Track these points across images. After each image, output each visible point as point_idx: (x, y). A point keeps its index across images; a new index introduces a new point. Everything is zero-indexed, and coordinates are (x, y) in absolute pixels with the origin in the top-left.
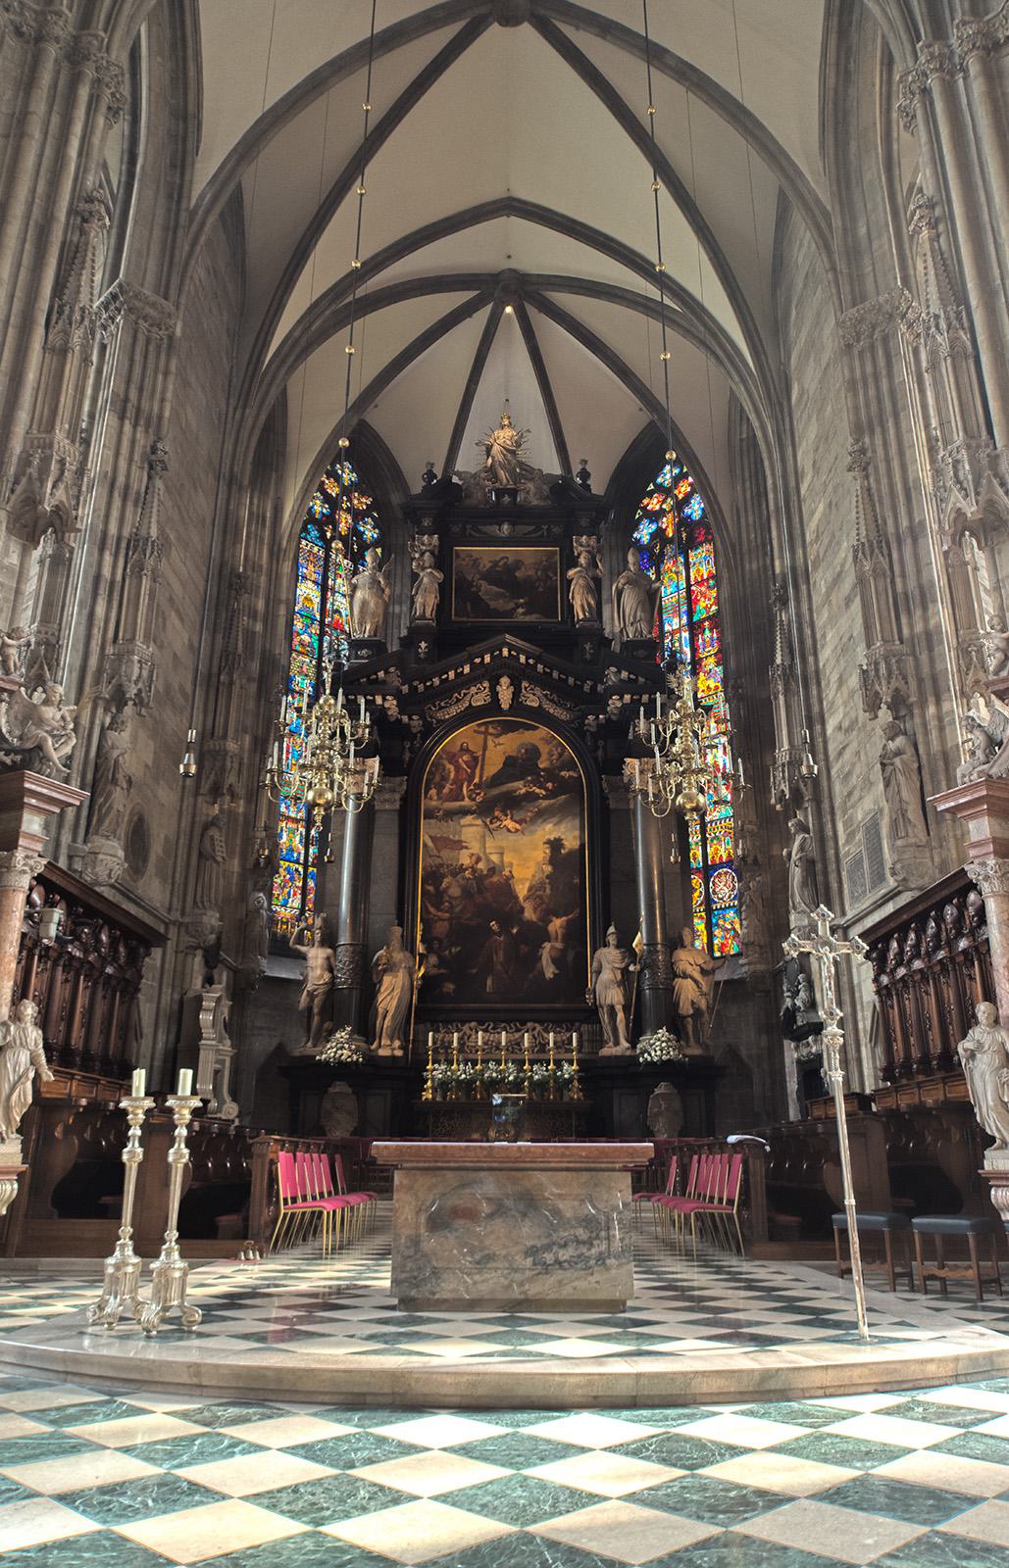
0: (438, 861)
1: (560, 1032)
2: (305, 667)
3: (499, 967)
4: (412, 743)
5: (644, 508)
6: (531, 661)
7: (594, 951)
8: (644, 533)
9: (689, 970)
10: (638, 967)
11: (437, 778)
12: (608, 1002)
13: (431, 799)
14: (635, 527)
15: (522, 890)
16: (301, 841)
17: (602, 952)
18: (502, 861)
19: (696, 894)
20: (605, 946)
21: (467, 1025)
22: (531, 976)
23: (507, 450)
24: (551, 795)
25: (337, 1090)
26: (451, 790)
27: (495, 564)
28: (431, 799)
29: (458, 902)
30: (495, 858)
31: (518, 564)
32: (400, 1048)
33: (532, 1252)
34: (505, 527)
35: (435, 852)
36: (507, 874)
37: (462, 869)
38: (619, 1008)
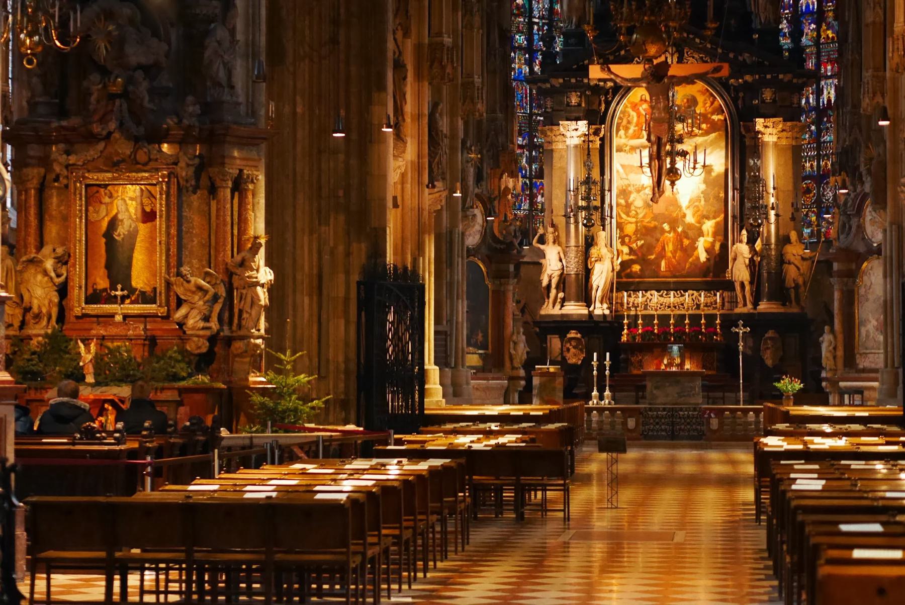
0: (626, 182)
1: (709, 297)
2: (521, 26)
3: (669, 255)
4: (606, 98)
6: (691, 36)
7: (733, 244)
9: (792, 259)
10: (759, 259)
11: (625, 122)
12: (740, 279)
13: (621, 138)
16: (526, 162)
17: (738, 245)
20: (741, 242)
21: (649, 292)
22: (691, 260)
24: (707, 133)
26: (635, 131)
28: (621, 138)
29: (641, 210)
32: (608, 308)
33: (677, 393)
35: (624, 176)
38: (746, 283)
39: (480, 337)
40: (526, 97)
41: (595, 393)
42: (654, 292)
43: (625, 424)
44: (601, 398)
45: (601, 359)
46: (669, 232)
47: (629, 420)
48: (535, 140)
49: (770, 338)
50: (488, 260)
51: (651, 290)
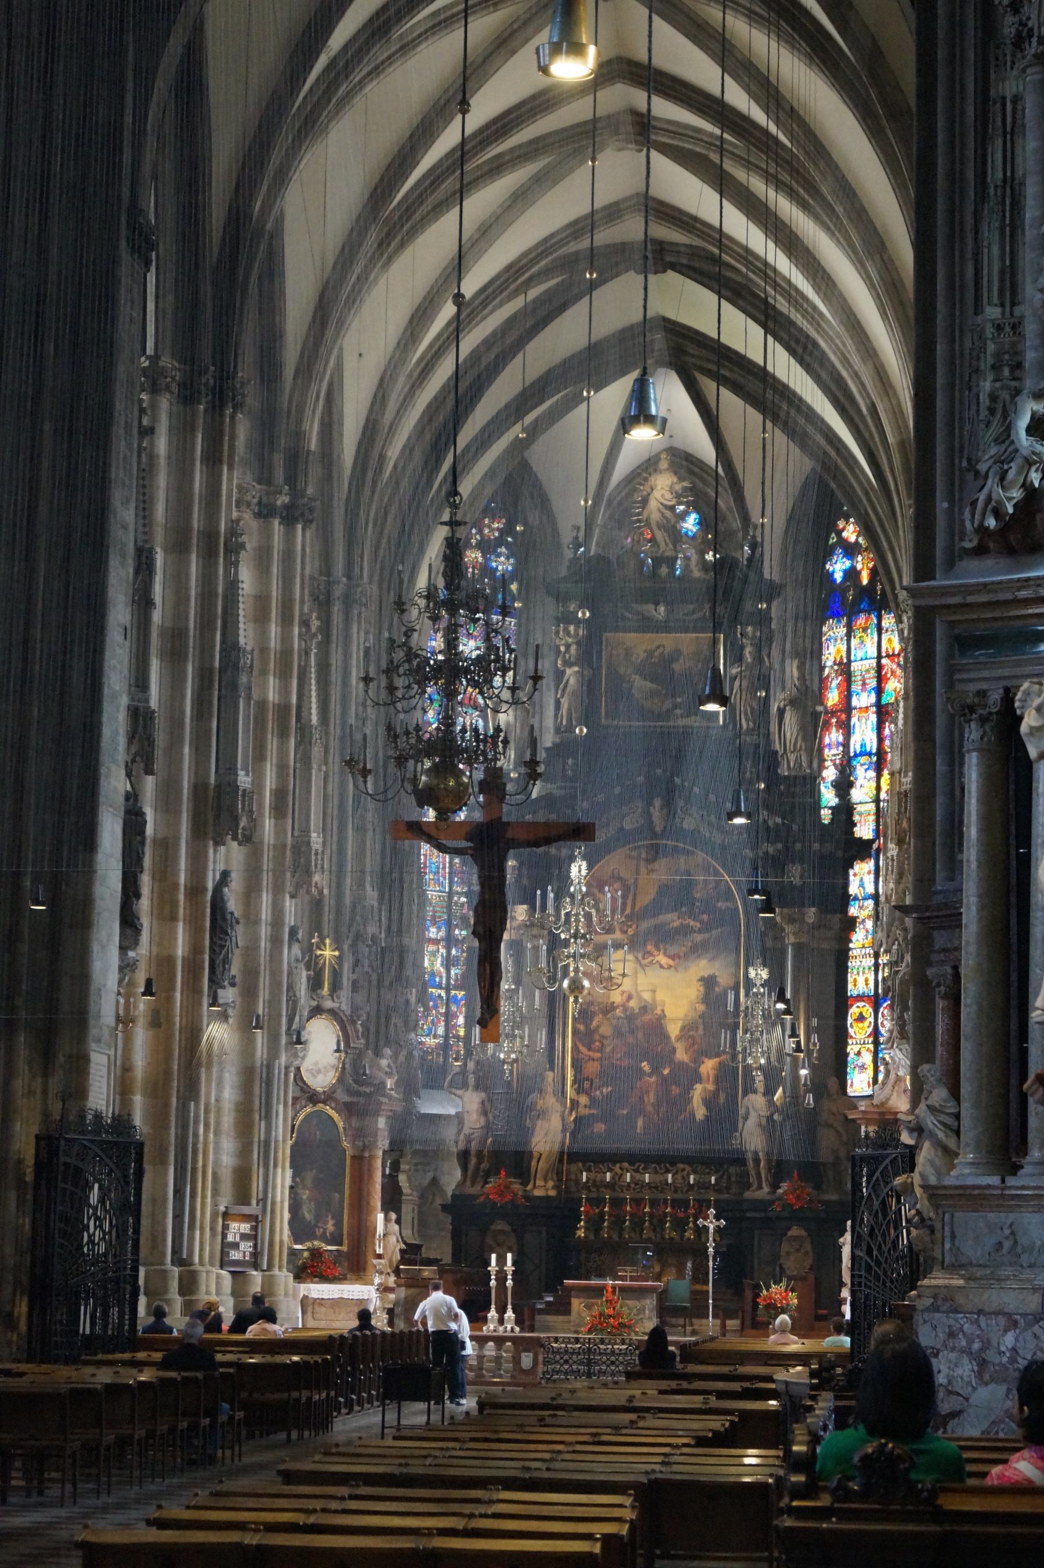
3: (649, 1108)
5: (839, 533)
7: (745, 1093)
8: (838, 567)
14: (828, 553)
15: (674, 1030)
17: (751, 1097)
18: (654, 999)
19: (866, 1024)
20: (755, 1092)
23: (666, 506)
24: (706, 928)
25: (499, 1227)
27: (650, 654)
30: (647, 996)
31: (676, 655)
34: (662, 609)
36: (658, 1011)
37: (613, 1007)
39: (330, 1226)
40: (444, 868)
41: (493, 1314)
42: (626, 1165)
43: (516, 1360)
44: (501, 1321)
45: (501, 1261)
46: (650, 1075)
47: (523, 1355)
48: (457, 932)
49: (796, 1238)
50: (349, 1110)
51: (620, 1162)
